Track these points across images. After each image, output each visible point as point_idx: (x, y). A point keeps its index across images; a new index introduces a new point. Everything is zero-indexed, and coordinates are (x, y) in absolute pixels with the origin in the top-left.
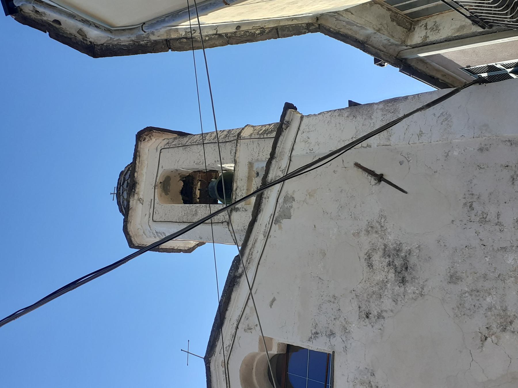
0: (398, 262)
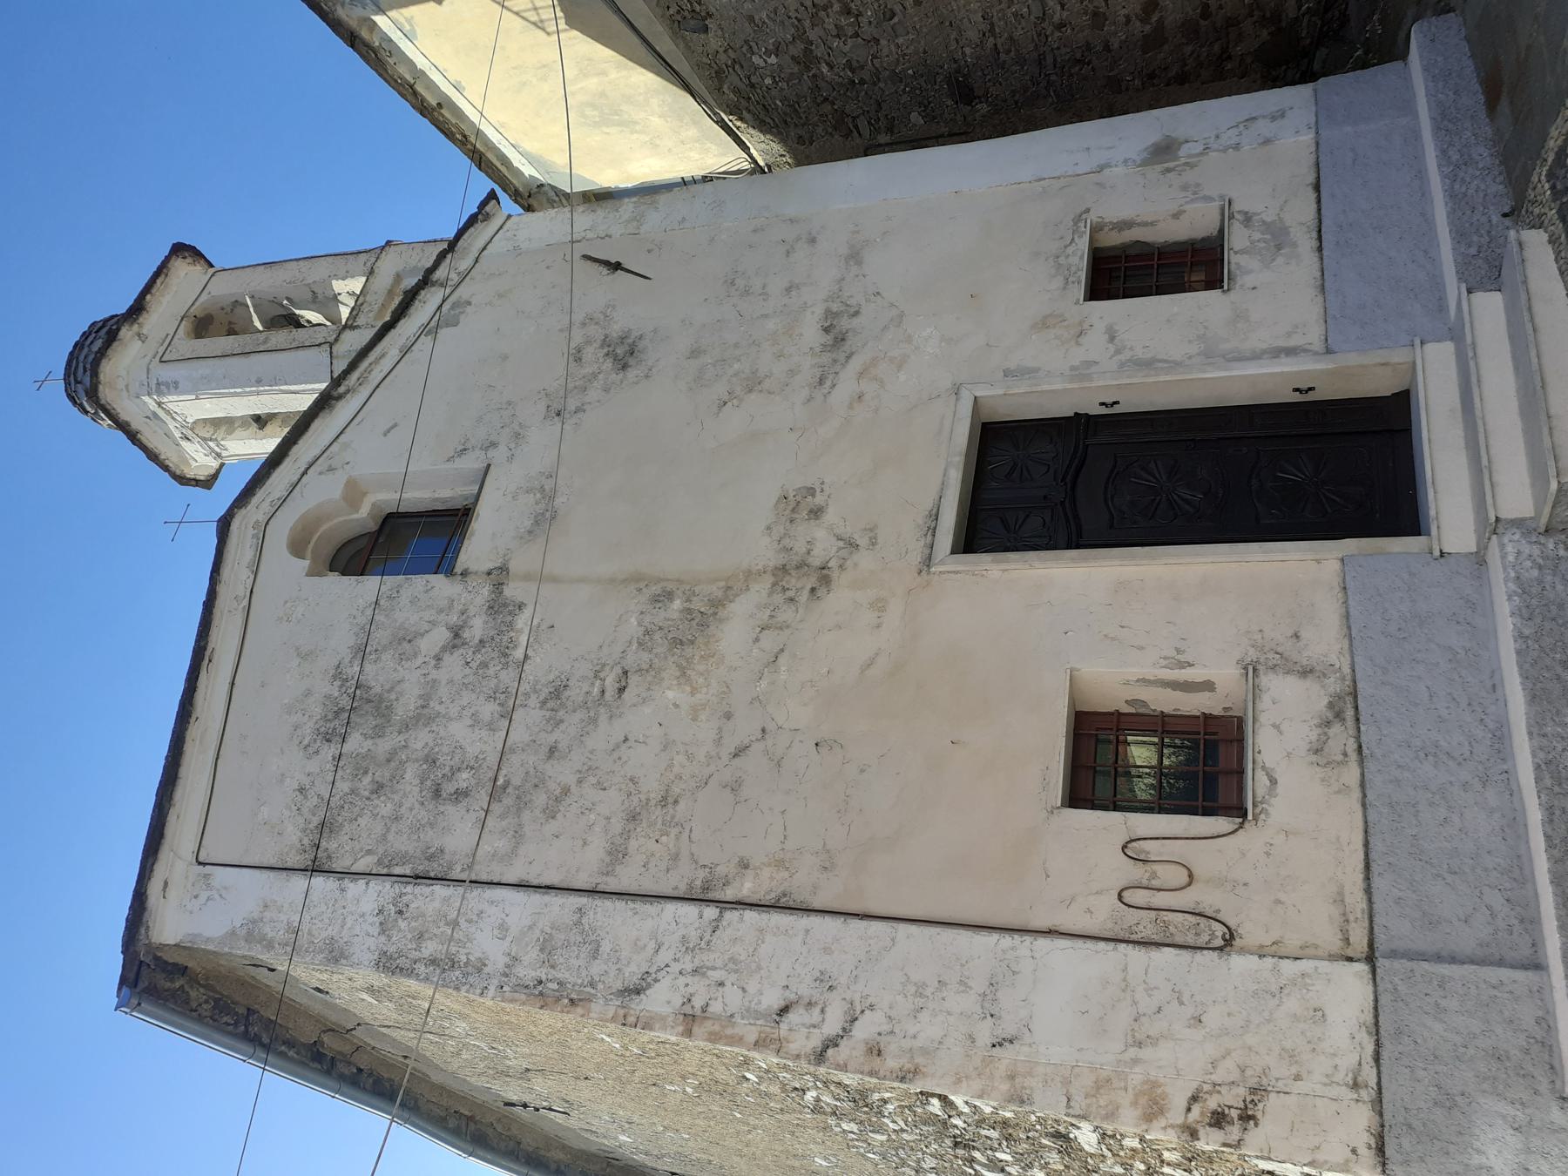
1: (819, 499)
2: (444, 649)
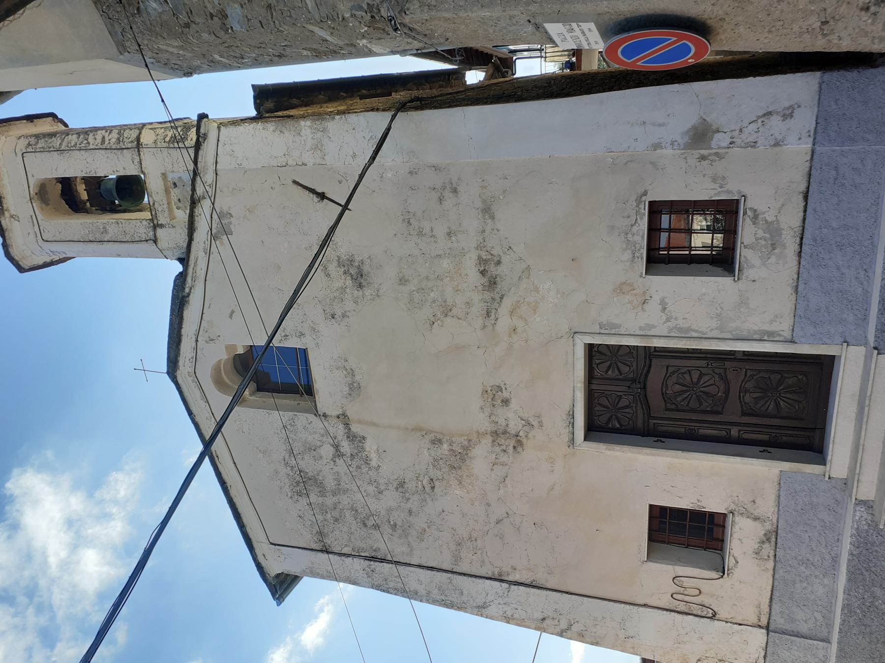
0: (353, 271)
1: (505, 394)
2: (334, 456)
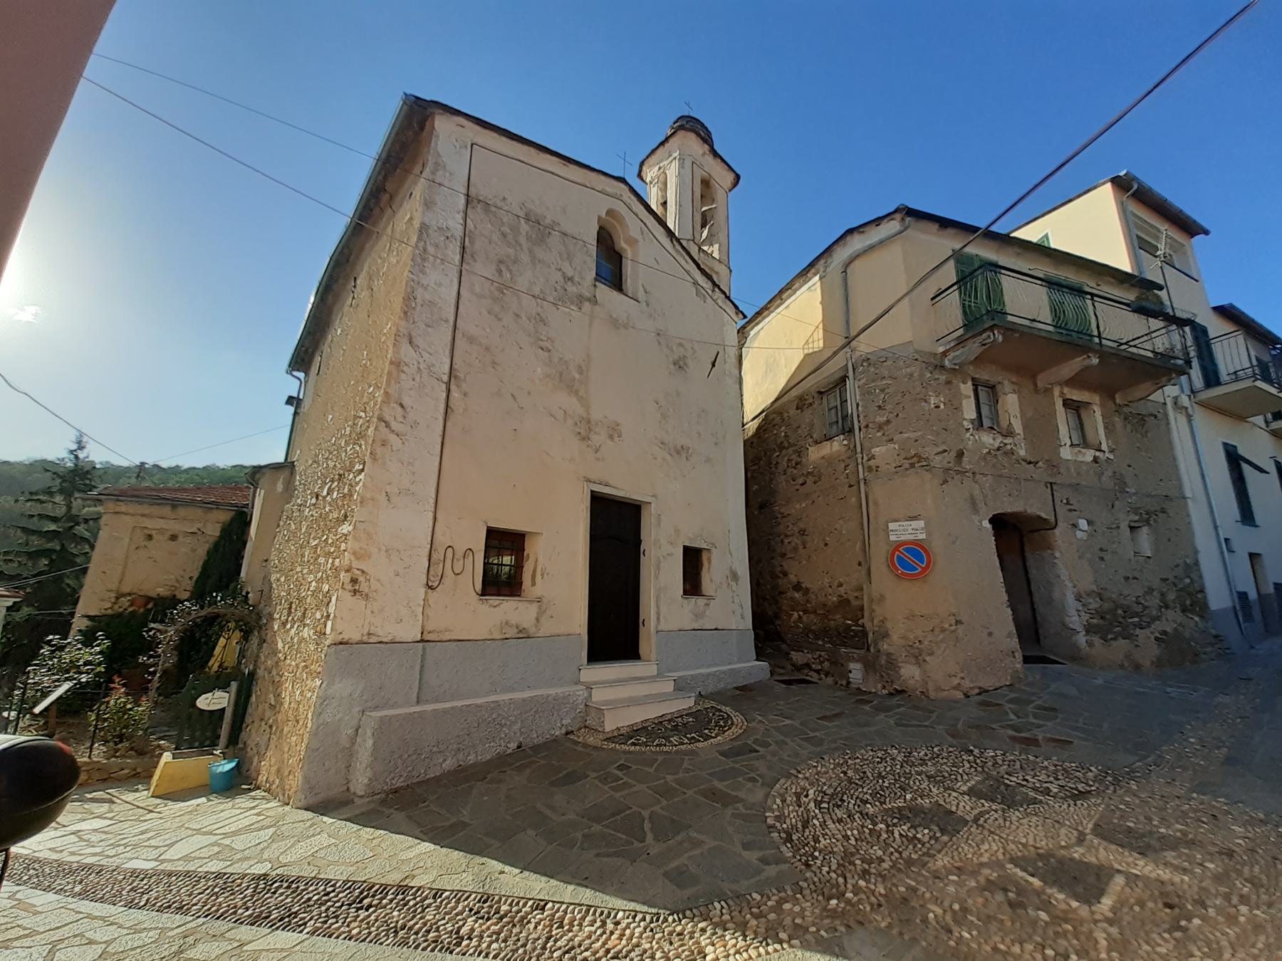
1: (616, 439)
